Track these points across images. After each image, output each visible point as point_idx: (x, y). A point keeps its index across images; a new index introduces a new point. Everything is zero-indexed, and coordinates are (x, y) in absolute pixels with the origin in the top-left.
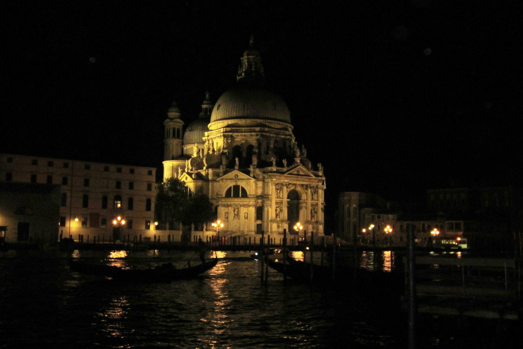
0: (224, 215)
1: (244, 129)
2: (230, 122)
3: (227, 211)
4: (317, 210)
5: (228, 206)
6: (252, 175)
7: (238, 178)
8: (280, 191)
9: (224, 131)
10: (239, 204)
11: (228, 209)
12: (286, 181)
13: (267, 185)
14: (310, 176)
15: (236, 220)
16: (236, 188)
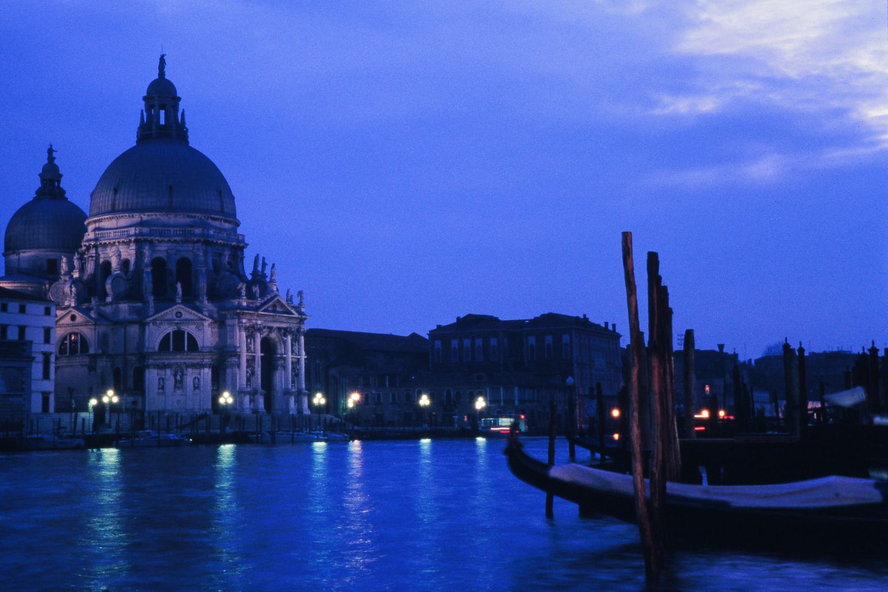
0: (157, 382)
1: (174, 230)
2: (145, 217)
3: (163, 377)
4: (298, 370)
5: (164, 367)
6: (206, 313)
7: (182, 318)
8: (251, 339)
9: (137, 232)
10: (185, 363)
11: (166, 373)
12: (259, 322)
13: (233, 331)
14: (292, 314)
15: (179, 392)
16: (179, 334)
